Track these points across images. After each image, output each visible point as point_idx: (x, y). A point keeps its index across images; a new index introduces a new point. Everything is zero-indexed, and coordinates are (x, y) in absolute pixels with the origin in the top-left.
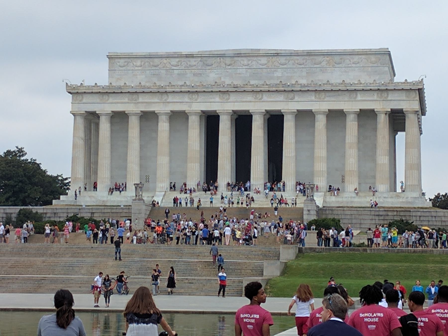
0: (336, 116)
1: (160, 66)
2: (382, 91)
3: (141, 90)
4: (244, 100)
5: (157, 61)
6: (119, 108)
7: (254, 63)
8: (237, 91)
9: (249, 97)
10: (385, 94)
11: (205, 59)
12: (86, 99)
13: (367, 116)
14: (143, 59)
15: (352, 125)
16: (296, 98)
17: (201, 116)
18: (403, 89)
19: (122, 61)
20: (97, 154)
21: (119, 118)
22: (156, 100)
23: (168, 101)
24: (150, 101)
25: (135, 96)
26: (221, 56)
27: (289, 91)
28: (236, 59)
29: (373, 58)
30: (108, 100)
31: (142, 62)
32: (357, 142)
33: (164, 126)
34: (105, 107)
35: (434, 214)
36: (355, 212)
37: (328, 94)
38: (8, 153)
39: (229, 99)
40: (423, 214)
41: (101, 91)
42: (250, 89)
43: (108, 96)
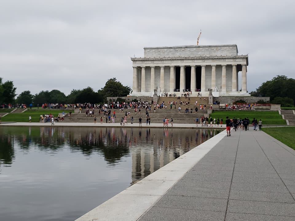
0: (219, 67)
2: (235, 58)
3: (155, 59)
5: (160, 50)
6: (148, 65)
8: (186, 59)
9: (190, 61)
10: (235, 60)
12: (137, 62)
13: (229, 67)
15: (224, 70)
17: (174, 68)
19: (149, 50)
20: (141, 80)
21: (148, 69)
24: (158, 63)
25: (153, 61)
27: (203, 59)
28: (185, 49)
29: (231, 48)
32: (225, 75)
33: (162, 71)
34: (143, 65)
35: (252, 98)
36: (226, 98)
37: (216, 60)
38: (111, 79)
40: (248, 99)
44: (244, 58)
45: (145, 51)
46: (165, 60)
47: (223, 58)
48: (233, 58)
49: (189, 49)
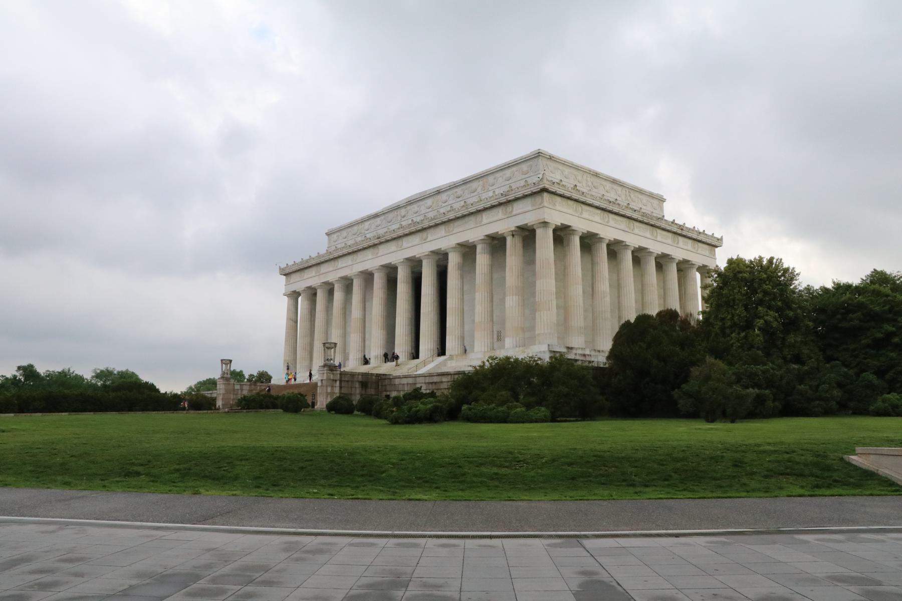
5: (355, 228)
7: (423, 208)
10: (509, 208)
12: (295, 277)
16: (430, 238)
18: (525, 197)
25: (318, 268)
28: (409, 208)
33: (338, 295)
44: (534, 194)
45: (329, 240)
47: (471, 214)
48: (500, 204)
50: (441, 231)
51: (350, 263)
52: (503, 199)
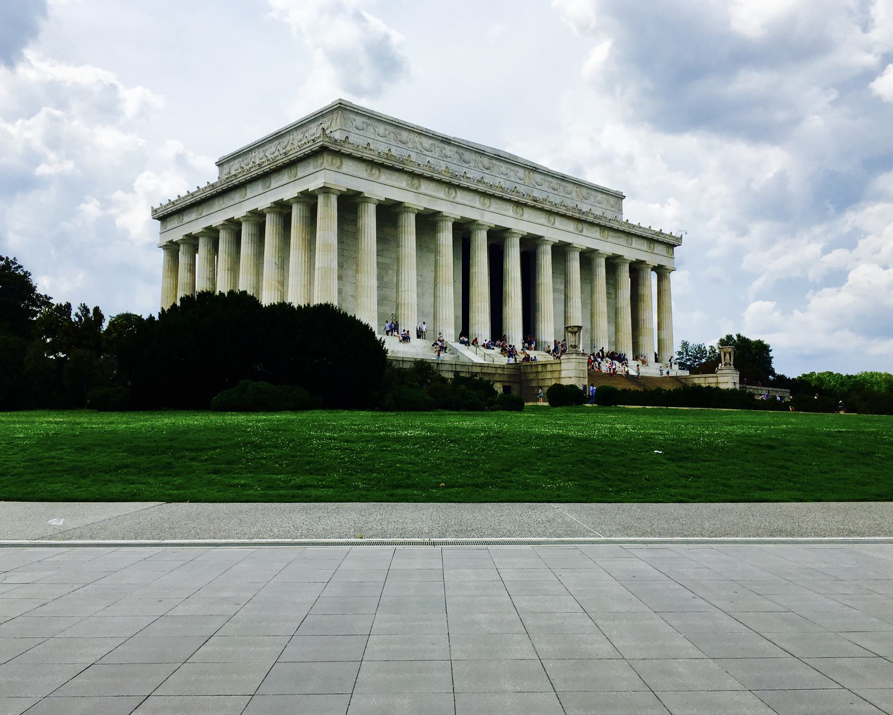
1: (410, 145)
4: (538, 221)
5: (405, 135)
11: (461, 151)
14: (387, 127)
16: (585, 232)
22: (442, 195)
23: (456, 200)
25: (416, 181)
26: (480, 152)
27: (580, 220)
28: (494, 161)
29: (612, 200)
30: (379, 177)
31: (385, 129)
37: (611, 234)
39: (522, 215)
41: (377, 159)
42: (547, 207)
43: (380, 171)
46: (467, 189)
49: (503, 167)
50: (596, 233)
51: (478, 205)
52: (656, 237)
